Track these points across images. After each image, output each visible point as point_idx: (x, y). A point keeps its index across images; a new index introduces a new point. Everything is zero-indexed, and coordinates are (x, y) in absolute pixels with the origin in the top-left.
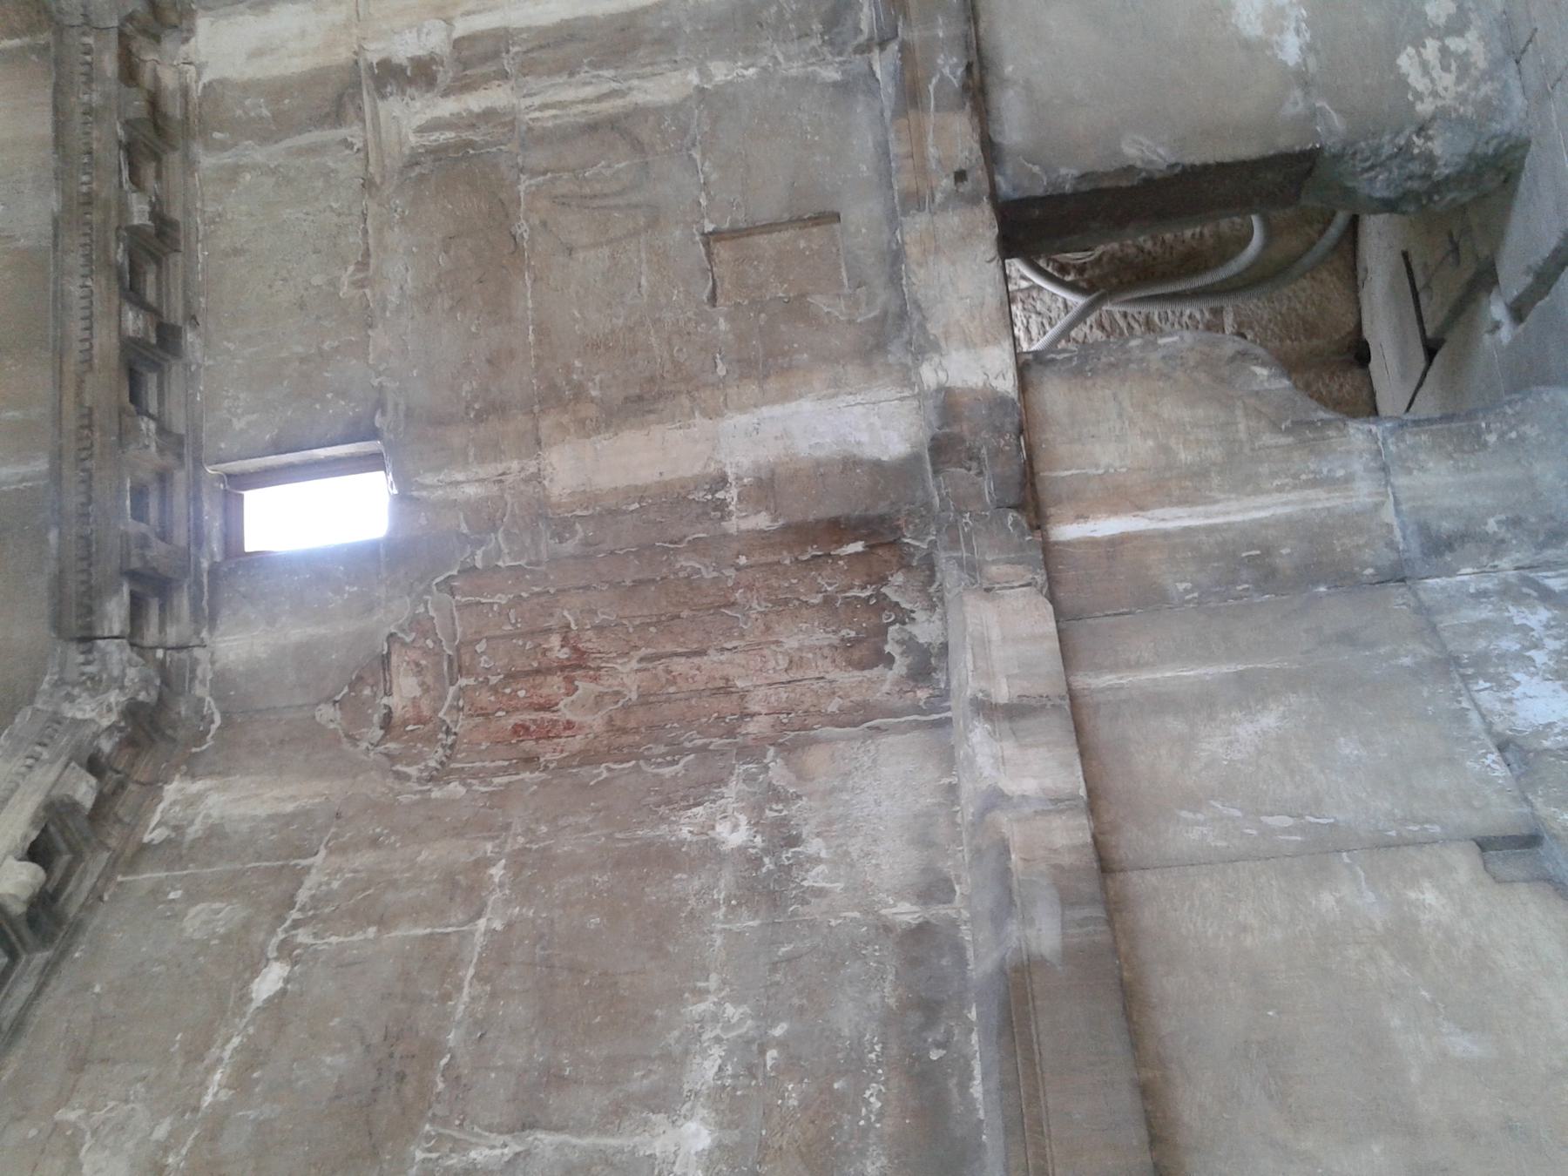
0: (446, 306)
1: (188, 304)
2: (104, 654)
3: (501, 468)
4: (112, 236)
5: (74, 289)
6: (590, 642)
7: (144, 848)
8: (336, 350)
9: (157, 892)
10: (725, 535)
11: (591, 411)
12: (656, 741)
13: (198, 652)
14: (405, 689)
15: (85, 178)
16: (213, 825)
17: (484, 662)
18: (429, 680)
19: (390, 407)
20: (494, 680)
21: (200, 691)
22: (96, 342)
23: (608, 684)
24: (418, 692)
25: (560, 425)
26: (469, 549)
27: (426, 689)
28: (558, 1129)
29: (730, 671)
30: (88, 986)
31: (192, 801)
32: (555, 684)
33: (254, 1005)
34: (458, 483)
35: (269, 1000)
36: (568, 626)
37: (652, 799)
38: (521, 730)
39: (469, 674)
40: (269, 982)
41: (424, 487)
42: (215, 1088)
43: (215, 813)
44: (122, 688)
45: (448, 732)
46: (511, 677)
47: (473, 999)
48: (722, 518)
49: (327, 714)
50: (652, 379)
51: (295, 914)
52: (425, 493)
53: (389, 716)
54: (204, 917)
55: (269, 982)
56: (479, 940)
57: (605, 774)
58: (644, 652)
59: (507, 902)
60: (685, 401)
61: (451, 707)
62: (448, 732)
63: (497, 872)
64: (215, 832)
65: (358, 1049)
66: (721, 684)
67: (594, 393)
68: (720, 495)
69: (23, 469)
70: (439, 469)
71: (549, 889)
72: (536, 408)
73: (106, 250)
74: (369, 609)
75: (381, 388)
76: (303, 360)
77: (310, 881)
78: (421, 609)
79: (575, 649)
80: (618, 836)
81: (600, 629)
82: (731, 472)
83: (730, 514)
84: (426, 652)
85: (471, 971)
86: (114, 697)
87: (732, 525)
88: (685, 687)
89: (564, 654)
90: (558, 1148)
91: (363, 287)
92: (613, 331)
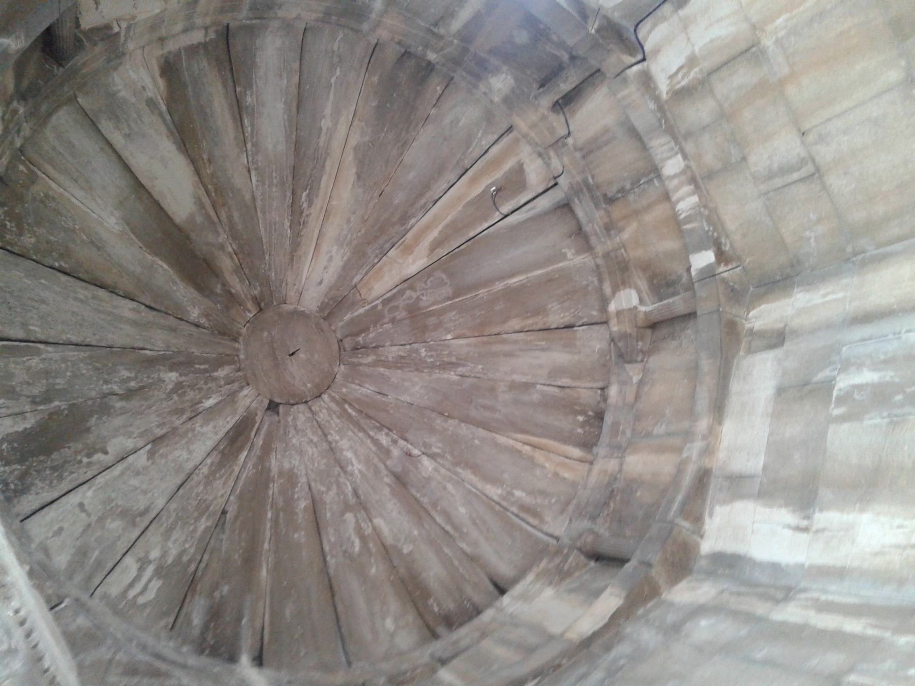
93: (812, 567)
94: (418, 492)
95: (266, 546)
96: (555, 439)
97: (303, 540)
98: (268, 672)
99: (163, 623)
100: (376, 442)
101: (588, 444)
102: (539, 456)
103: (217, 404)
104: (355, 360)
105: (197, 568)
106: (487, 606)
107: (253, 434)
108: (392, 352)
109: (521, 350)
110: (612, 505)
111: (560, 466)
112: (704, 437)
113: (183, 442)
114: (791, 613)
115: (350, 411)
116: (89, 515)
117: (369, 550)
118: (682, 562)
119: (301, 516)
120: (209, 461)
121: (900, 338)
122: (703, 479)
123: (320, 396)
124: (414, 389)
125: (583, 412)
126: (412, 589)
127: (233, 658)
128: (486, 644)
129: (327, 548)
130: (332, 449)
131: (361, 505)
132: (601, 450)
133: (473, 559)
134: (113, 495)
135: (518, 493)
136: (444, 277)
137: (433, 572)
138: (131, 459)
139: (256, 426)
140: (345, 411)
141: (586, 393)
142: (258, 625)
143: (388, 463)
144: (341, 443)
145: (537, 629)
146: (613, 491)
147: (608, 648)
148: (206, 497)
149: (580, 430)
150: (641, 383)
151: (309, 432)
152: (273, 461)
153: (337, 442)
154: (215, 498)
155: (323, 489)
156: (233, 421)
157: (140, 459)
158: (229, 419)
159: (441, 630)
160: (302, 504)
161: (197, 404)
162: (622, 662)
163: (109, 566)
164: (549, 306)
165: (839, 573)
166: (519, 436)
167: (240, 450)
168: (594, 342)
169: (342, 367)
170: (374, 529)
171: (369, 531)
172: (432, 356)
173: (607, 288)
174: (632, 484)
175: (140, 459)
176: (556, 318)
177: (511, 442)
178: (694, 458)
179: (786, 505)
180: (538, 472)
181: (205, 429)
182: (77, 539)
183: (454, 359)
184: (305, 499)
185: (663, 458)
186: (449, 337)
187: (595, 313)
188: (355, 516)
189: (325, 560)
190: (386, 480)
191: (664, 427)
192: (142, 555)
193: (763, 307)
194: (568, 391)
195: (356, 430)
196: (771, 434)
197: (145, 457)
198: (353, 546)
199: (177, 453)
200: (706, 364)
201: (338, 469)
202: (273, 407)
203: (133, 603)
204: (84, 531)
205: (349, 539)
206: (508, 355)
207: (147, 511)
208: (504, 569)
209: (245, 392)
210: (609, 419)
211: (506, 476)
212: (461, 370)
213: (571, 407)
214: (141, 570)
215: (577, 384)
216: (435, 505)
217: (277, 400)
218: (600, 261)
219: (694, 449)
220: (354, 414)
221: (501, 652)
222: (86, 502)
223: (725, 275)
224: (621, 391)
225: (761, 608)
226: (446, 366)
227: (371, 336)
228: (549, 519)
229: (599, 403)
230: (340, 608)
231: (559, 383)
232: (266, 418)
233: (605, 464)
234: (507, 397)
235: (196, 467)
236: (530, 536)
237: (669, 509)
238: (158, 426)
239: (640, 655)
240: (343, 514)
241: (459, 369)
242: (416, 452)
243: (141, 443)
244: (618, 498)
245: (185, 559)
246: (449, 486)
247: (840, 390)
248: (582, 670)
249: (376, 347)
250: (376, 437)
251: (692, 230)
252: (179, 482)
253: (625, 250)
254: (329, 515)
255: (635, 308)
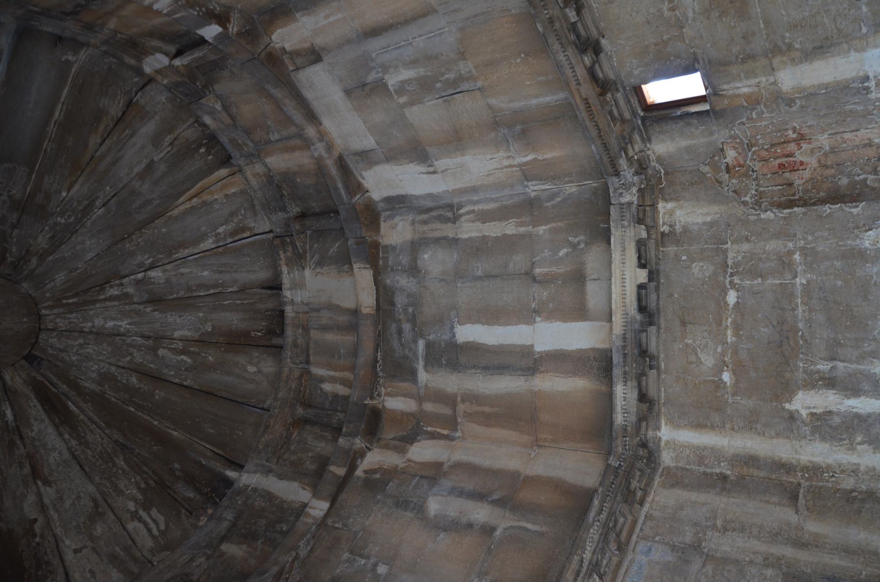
0: (717, 15)
1: (597, 28)
2: (624, 176)
3: (757, 80)
4: (567, 32)
5: (561, 57)
6: (805, 131)
7: (663, 234)
8: (670, 39)
9: (677, 257)
10: (869, 99)
11: (797, 54)
12: (841, 173)
13: (648, 152)
14: (731, 155)
15: (546, 12)
16: (684, 226)
17: (760, 141)
18: (740, 151)
19: (701, 60)
20: (766, 147)
21: (653, 164)
22: (578, 74)
23: (814, 144)
24: (736, 155)
25: (782, 61)
26: (749, 112)
27: (740, 154)
28: (843, 361)
29: (871, 136)
30: (671, 295)
31: (671, 213)
32: (792, 147)
33: (731, 306)
34: (739, 88)
35: (735, 305)
36: (795, 127)
37: (851, 225)
38: (781, 166)
39: (755, 146)
40: (732, 297)
41: (724, 90)
42: (730, 338)
43: (682, 219)
44: (634, 185)
45: (753, 171)
46: (772, 145)
47: (804, 311)
48: (867, 93)
49: (706, 169)
50: (827, 38)
51: (730, 270)
52: (725, 93)
53: (728, 166)
54: (698, 268)
55: (732, 297)
56: (799, 288)
57: (829, 211)
58: (830, 132)
59: (805, 271)
60: (845, 46)
61: (751, 159)
62: (753, 171)
63: (797, 257)
64: (686, 230)
65: (770, 327)
66: (867, 142)
67: (797, 46)
68: (866, 84)
69: (555, 97)
70: (730, 83)
71: (819, 267)
72: (770, 55)
73: (567, 37)
74: (712, 134)
75: (694, 53)
76: (656, 45)
77: (731, 255)
78: (733, 132)
79: (799, 134)
80: (841, 243)
81: (810, 127)
82: (871, 75)
83: (871, 92)
84: (737, 143)
85: (800, 301)
86: (634, 190)
87: (873, 96)
88: (850, 144)
89: (794, 136)
90: (845, 367)
91: (674, 10)
92: (804, 18)
93: (454, 191)
94: (172, 294)
95: (156, 423)
96: (203, 179)
97: (162, 394)
98: (248, 467)
99: (184, 518)
100: (112, 298)
101: (226, 160)
102: (206, 197)
103: (13, 409)
104: (26, 272)
105: (152, 478)
106: (282, 304)
107: (53, 389)
108: (42, 241)
109: (120, 151)
110: (285, 192)
111: (221, 189)
112: (321, 140)
113: (43, 452)
114: (468, 230)
115: (70, 301)
116: (85, 547)
117: (193, 352)
118: (371, 215)
119: (142, 386)
120: (67, 436)
121: (411, 44)
122: (342, 164)
123: (40, 317)
124: (88, 246)
125: (200, 146)
126: (237, 341)
127: (229, 483)
128: (314, 334)
129: (177, 381)
130: (97, 334)
131: (159, 339)
132: (239, 160)
133: (243, 289)
134: (74, 524)
135: (221, 230)
136: (6, 165)
137: (234, 320)
138: (46, 501)
139: (47, 383)
140: (68, 304)
141: (188, 132)
142: (209, 454)
143: (135, 300)
144: (96, 324)
145: (332, 307)
146: (277, 185)
147: (393, 304)
148: (98, 450)
149: (210, 158)
150: (225, 108)
151: (70, 342)
152: (87, 385)
153: (93, 327)
154: (102, 444)
155: (129, 358)
156: (35, 401)
157: (49, 493)
158: (31, 404)
159: (276, 341)
160: (134, 380)
161: (8, 426)
162: (410, 310)
163: (130, 542)
164: (101, 105)
165: (474, 190)
166: (181, 200)
167: (66, 408)
168: (157, 99)
169: (25, 285)
170: (180, 340)
171: (180, 345)
172: (69, 216)
173: (132, 62)
174: (288, 177)
175: (49, 493)
176: (115, 109)
177: (182, 208)
178: (325, 155)
179: (412, 162)
180: (216, 206)
181: (35, 428)
182: (102, 560)
183: (86, 202)
184: (131, 376)
185: (297, 154)
186: (64, 194)
187: (136, 80)
188: (164, 348)
189: (186, 387)
190: (148, 310)
191: (276, 134)
192: (129, 515)
193: (279, 31)
194: (176, 143)
195: (92, 307)
196: (365, 122)
197: (48, 488)
198: (185, 362)
199: (51, 460)
200: (278, 93)
201: (118, 338)
202: (30, 358)
203: (163, 533)
204: (97, 554)
205: (178, 361)
206: (115, 162)
207: (94, 501)
208: (263, 275)
209: (7, 377)
210: (224, 139)
211: (203, 229)
212: (98, 203)
213: (188, 150)
214: (140, 520)
215: (177, 132)
216: (189, 289)
217: (27, 351)
218: (104, 48)
219: (320, 149)
220: (75, 300)
221: (331, 337)
222: (74, 547)
223: (235, 29)
224: (214, 119)
225: (448, 230)
226: (88, 209)
227: (14, 250)
228: (253, 224)
229: (203, 131)
230: (224, 395)
231: (166, 144)
232: (42, 371)
233: (253, 171)
234: (147, 186)
235: (69, 449)
236: (253, 244)
237: (340, 195)
238: (21, 466)
239: (415, 301)
240: (156, 355)
241: (97, 203)
242: (140, 276)
243: (34, 487)
244: (284, 186)
245: (143, 485)
246: (183, 270)
247: (393, 85)
248: (394, 327)
249: (27, 251)
250: (108, 295)
251: (182, 17)
252: (78, 468)
253: (121, 33)
254: (152, 365)
255: (171, 66)
